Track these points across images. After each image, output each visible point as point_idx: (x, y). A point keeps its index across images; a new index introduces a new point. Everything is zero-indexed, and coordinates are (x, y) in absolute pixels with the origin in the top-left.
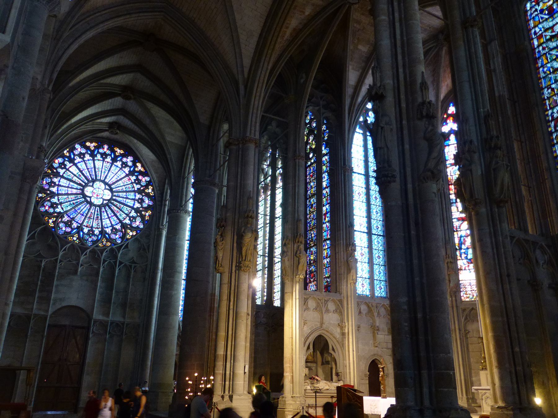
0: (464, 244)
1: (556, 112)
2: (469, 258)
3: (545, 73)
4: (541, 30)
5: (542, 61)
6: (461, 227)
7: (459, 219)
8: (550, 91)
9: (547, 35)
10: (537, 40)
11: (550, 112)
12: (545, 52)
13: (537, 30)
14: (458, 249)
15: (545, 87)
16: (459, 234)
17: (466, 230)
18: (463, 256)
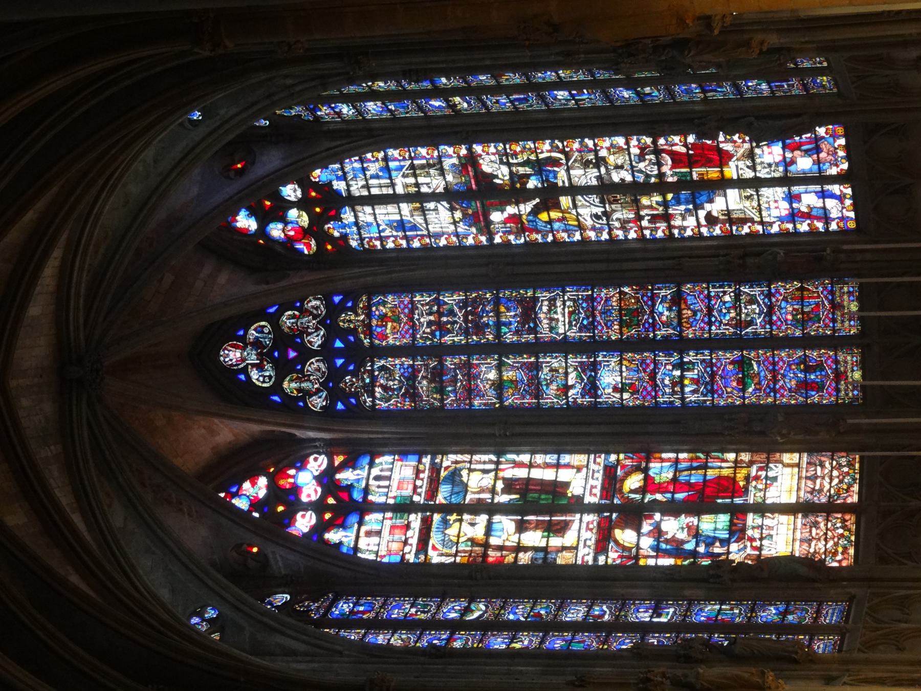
0: (683, 542)
2: (727, 536)
6: (626, 544)
7: (601, 547)
14: (692, 560)
16: (646, 554)
17: (639, 534)
18: (717, 550)
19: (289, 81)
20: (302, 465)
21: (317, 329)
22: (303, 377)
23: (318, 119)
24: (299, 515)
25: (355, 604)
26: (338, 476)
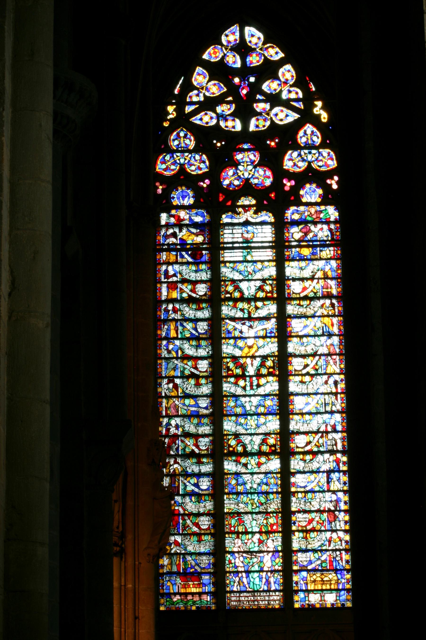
1: (173, 425)
3: (169, 352)
4: (175, 275)
5: (167, 329)
8: (171, 385)
9: (184, 291)
10: (168, 287)
11: (165, 420)
12: (176, 318)
13: (171, 273)
15: (166, 377)
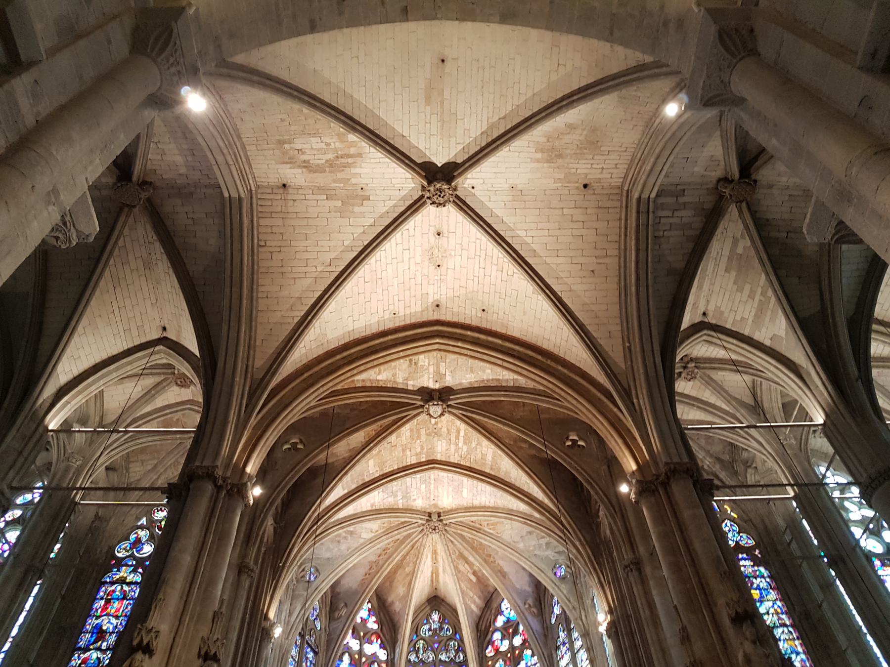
19: (583, 618)
20: (382, 646)
21: (449, 658)
22: (424, 652)
23: (558, 648)
24: (358, 641)
25: (311, 662)
26: (376, 664)
